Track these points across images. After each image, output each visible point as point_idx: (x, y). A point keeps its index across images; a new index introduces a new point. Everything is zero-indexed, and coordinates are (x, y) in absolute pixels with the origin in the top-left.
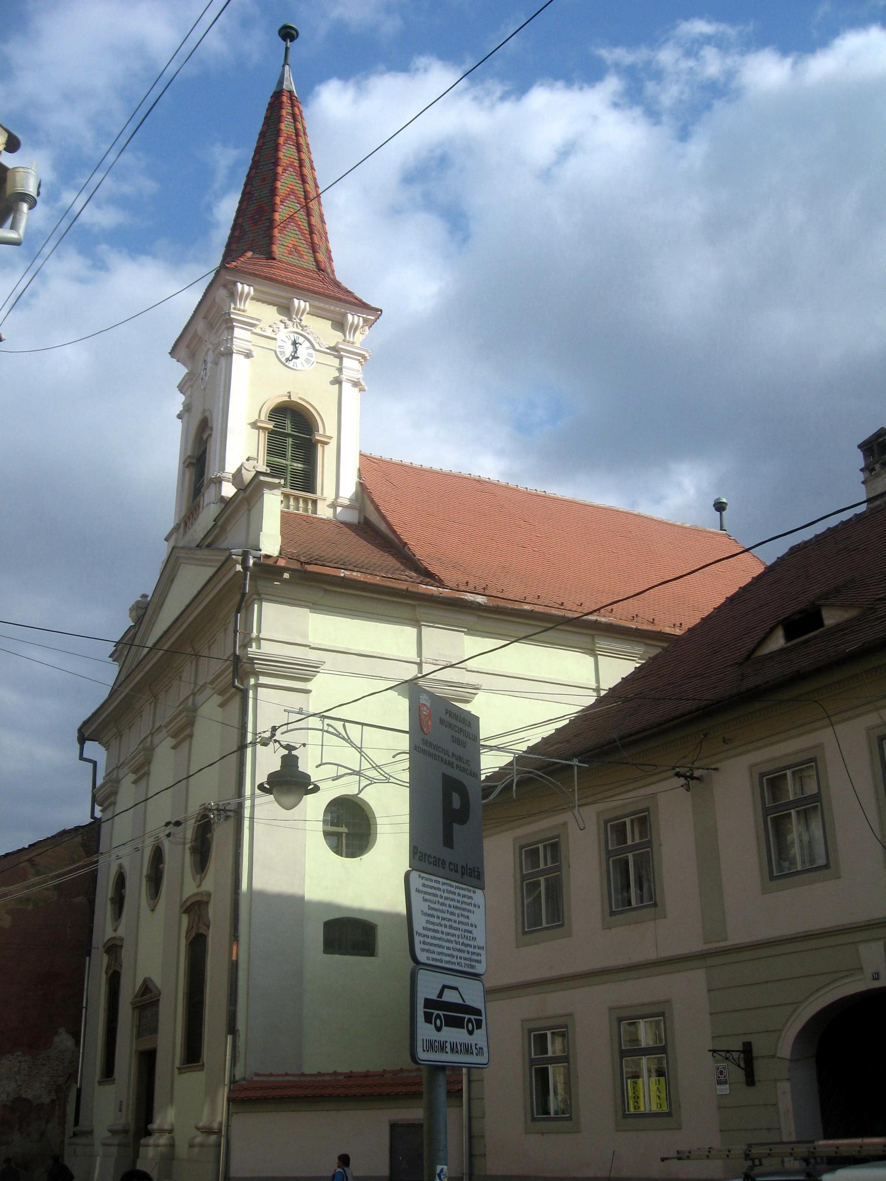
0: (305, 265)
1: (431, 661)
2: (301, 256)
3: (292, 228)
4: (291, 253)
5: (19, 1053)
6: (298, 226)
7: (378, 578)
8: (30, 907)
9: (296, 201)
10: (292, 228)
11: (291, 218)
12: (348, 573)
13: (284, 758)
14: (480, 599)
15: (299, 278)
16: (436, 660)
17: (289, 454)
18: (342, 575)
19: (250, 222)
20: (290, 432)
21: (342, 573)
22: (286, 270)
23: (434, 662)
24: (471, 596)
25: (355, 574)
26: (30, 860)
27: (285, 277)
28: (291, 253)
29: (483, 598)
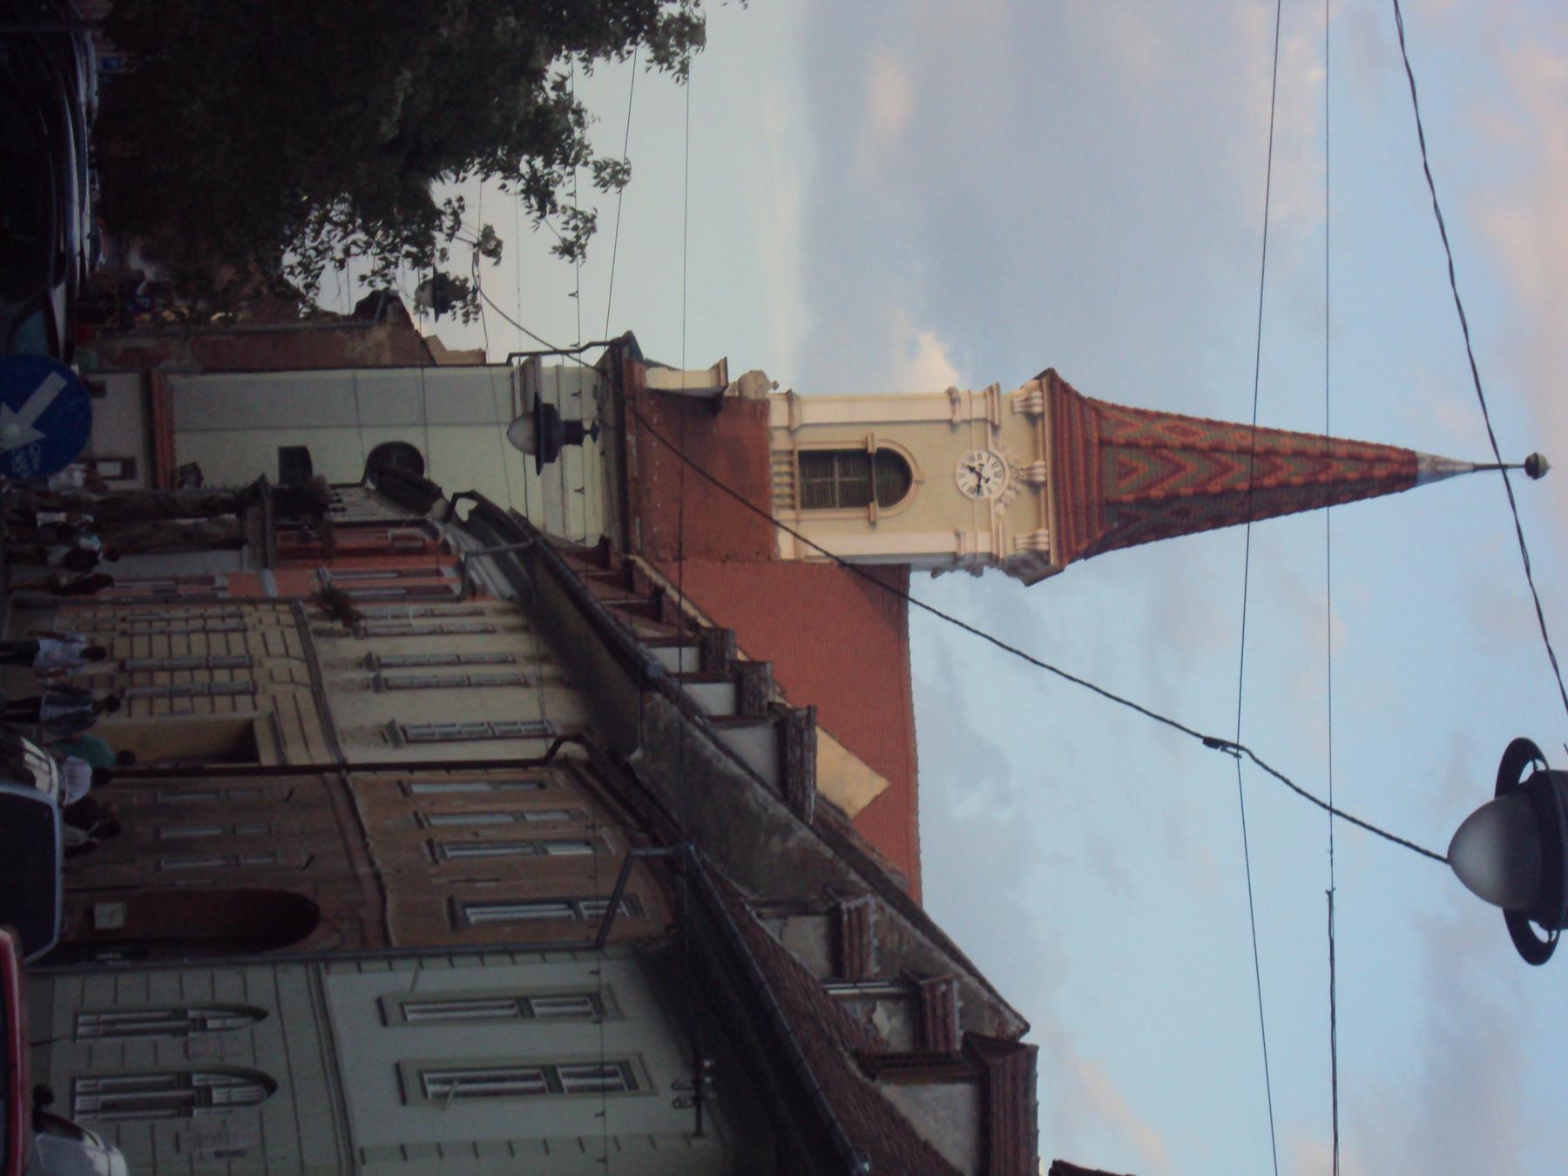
2: (1122, 477)
4: (1122, 464)
11: (1179, 468)
17: (846, 479)
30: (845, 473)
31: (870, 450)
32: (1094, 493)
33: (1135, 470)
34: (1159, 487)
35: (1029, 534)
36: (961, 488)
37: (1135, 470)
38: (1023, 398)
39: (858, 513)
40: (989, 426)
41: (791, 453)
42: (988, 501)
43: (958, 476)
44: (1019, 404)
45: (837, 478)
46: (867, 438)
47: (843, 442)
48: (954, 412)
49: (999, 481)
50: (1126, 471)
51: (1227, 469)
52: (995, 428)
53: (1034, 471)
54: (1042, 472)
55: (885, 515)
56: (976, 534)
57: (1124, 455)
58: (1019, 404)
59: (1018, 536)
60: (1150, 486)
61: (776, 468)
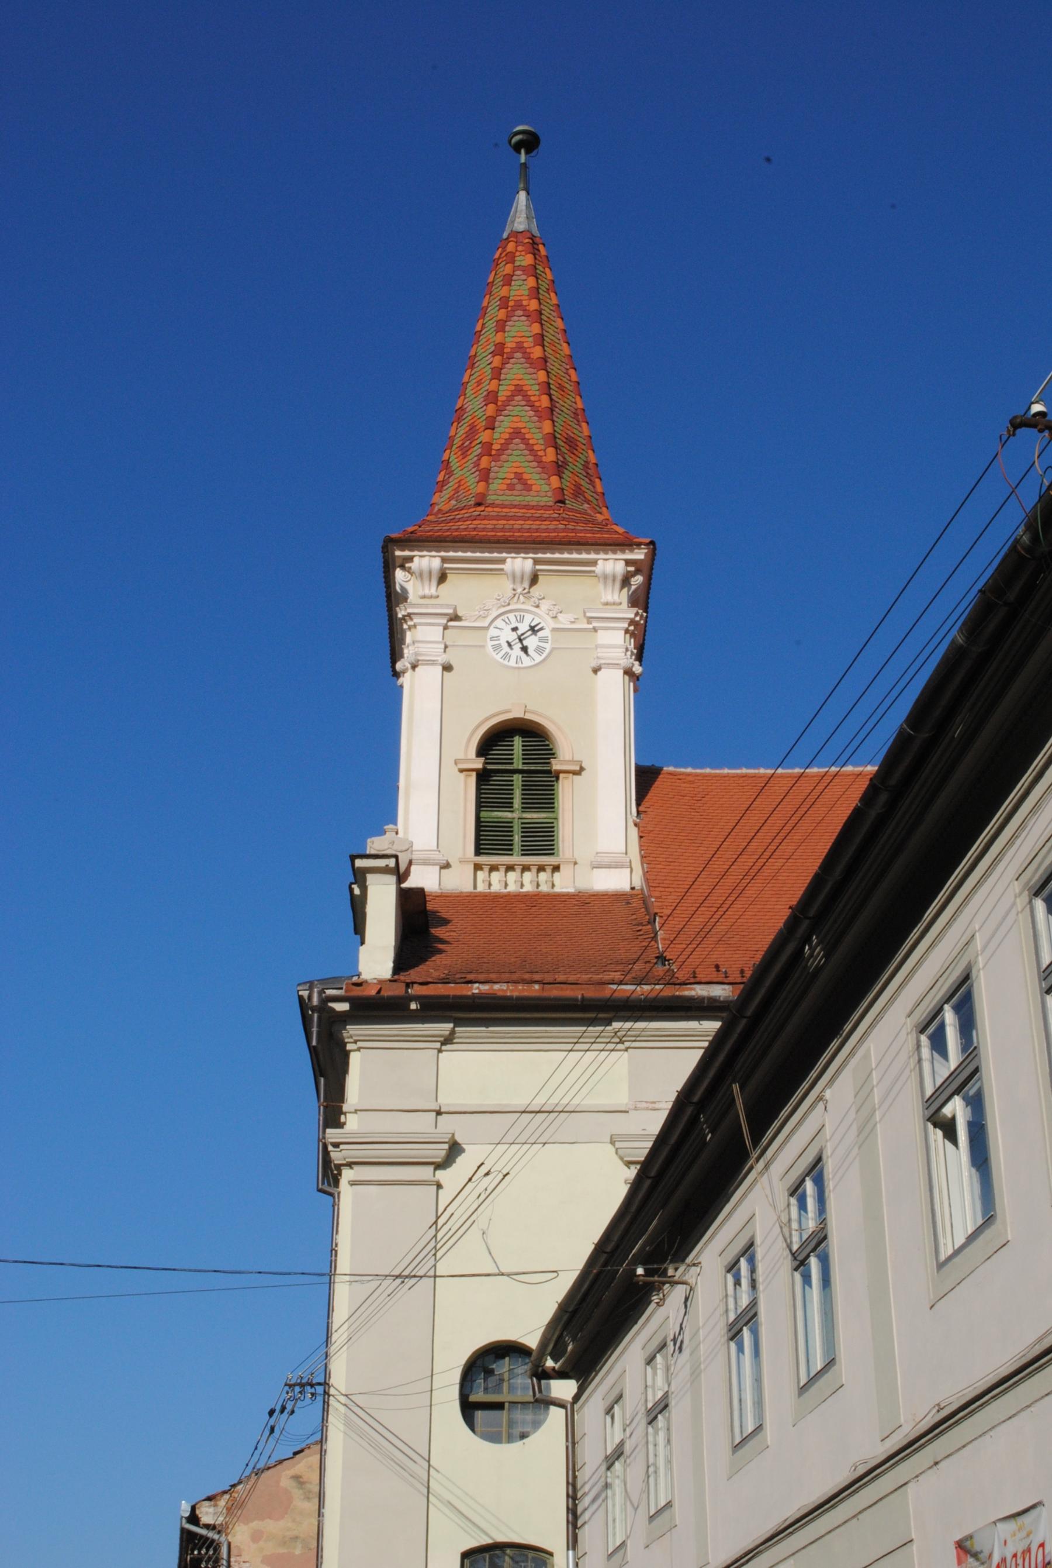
0: (531, 499)
1: (644, 1105)
2: (528, 487)
3: (515, 447)
4: (511, 487)
6: (525, 441)
7: (537, 987)
8: (298, 1552)
9: (524, 403)
10: (515, 447)
11: (517, 433)
12: (485, 988)
16: (654, 1103)
17: (517, 803)
18: (476, 991)
19: (460, 453)
20: (520, 767)
21: (476, 989)
22: (498, 518)
23: (651, 1106)
24: (701, 990)
25: (497, 987)
26: (297, 1478)
28: (511, 487)
29: (725, 989)
30: (508, 805)
32: (547, 514)
33: (519, 476)
35: (601, 586)
36: (536, 662)
39: (566, 791)
41: (478, 867)
42: (554, 630)
43: (520, 665)
45: (516, 815)
46: (461, 771)
47: (466, 799)
48: (433, 663)
50: (520, 481)
51: (519, 390)
52: (456, 618)
53: (518, 574)
54: (520, 563)
55: (566, 753)
56: (597, 647)
58: (427, 583)
59: (604, 600)
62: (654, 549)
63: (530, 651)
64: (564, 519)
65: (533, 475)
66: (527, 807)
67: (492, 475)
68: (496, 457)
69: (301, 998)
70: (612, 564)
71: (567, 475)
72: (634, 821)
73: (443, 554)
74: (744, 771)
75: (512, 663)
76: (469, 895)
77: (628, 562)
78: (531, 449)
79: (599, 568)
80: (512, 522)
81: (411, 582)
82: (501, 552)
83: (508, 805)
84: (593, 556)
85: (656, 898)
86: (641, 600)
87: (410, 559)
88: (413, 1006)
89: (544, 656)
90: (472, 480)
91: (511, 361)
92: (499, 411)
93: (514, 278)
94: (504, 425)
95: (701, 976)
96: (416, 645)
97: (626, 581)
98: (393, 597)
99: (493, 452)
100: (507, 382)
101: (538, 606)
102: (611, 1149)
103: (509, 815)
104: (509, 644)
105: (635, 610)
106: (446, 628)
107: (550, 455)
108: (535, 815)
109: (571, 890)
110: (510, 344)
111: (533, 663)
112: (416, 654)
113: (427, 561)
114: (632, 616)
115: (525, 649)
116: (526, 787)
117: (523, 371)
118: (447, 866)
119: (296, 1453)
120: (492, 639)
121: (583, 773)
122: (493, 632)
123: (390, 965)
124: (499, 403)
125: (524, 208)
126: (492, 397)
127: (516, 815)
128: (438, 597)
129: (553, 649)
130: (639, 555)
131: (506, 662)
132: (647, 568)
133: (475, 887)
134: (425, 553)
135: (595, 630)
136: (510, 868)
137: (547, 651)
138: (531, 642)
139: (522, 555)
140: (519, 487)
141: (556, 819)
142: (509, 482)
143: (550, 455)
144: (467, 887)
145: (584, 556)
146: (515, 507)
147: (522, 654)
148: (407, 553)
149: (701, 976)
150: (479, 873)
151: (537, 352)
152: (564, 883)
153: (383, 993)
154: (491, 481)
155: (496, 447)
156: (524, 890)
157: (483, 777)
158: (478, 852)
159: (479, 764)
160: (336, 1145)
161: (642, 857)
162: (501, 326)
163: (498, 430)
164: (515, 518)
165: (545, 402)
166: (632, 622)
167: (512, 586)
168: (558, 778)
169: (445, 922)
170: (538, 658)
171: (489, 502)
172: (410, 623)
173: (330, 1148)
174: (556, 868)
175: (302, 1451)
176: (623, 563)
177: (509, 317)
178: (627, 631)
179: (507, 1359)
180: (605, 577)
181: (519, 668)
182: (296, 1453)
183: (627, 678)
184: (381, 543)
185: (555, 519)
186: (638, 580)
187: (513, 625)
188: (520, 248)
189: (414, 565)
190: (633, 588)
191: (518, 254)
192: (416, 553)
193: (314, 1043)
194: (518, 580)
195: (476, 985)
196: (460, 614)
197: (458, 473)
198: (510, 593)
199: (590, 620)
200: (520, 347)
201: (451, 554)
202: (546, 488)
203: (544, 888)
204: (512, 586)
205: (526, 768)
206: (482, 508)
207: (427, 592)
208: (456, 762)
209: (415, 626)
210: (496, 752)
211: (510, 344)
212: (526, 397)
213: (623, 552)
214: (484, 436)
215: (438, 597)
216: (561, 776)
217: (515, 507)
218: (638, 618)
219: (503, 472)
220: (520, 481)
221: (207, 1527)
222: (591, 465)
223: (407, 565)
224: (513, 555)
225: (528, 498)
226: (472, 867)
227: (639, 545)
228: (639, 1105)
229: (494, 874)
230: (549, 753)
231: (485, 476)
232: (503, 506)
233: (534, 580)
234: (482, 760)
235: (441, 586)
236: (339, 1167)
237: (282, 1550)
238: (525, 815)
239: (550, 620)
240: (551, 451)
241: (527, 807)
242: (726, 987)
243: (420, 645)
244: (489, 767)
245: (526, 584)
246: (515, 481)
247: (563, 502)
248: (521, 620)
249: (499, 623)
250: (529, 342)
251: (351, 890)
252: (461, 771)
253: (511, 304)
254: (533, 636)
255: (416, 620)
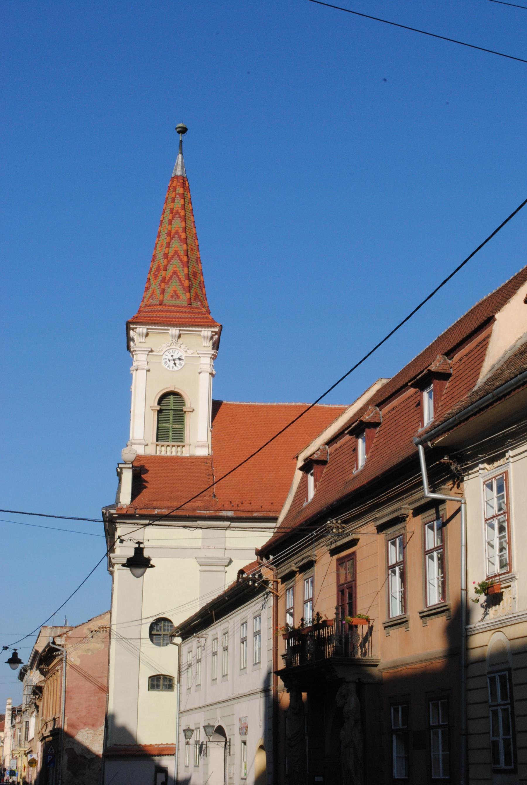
0: (179, 303)
1: (206, 547)
2: (178, 297)
4: (172, 297)
5: (87, 729)
6: (178, 276)
8: (90, 654)
11: (175, 273)
12: (159, 511)
13: (13, 653)
14: (230, 514)
15: (174, 315)
17: (171, 421)
20: (173, 408)
22: (167, 311)
25: (163, 510)
27: (165, 317)
30: (168, 422)
31: (159, 409)
33: (175, 292)
34: (183, 282)
35: (203, 340)
36: (179, 368)
37: (175, 292)
38: (138, 336)
39: (188, 418)
40: (150, 353)
41: (157, 445)
42: (186, 357)
43: (173, 370)
44: (141, 339)
45: (170, 426)
46: (152, 410)
47: (154, 421)
48: (143, 369)
49: (177, 351)
50: (175, 295)
51: (176, 253)
52: (152, 351)
53: (174, 335)
54: (174, 331)
55: (189, 404)
56: (200, 364)
57: (167, 296)
58: (141, 339)
60: (182, 285)
61: (163, 454)
62: (222, 328)
63: (177, 364)
64: (191, 313)
65: (181, 292)
66: (175, 422)
67: (165, 291)
68: (167, 283)
69: (103, 512)
70: (207, 332)
71: (193, 290)
72: (210, 430)
73: (147, 327)
74: (251, 403)
75: (171, 369)
76: (155, 456)
77: (212, 332)
78: (179, 279)
79: (202, 333)
80: (172, 314)
81: (136, 336)
82: (168, 327)
83: (168, 422)
84: (200, 329)
85: (215, 468)
86: (216, 346)
87: (136, 328)
88: (137, 516)
89: (182, 366)
90: (158, 292)
91: (174, 239)
92: (169, 262)
93: (176, 198)
94: (171, 269)
95: (226, 507)
96: (137, 362)
97: (211, 338)
98: (129, 339)
99: (166, 281)
100: (173, 249)
101: (180, 347)
102: (195, 560)
103: (168, 425)
104: (169, 360)
105: (214, 351)
106: (148, 355)
107: (186, 283)
108: (177, 426)
109: (188, 455)
110: (173, 231)
111: (178, 369)
112: (138, 366)
113: (142, 329)
114: (213, 353)
115: (175, 364)
116: (174, 415)
117: (178, 244)
118: (147, 445)
119: (89, 621)
120: (164, 359)
121: (194, 412)
122: (164, 357)
123: (130, 500)
124: (169, 259)
125: (181, 163)
126: (166, 256)
127: (170, 426)
128: (145, 342)
129: (185, 364)
130: (217, 329)
131: (168, 369)
132: (219, 333)
133: (156, 453)
134: (141, 326)
135: (200, 357)
136: (168, 446)
137: (183, 365)
138: (177, 362)
139: (175, 328)
140: (175, 297)
141: (184, 427)
142: (171, 294)
143: (186, 283)
144: (153, 454)
145: (197, 329)
146: (173, 306)
147: (174, 365)
148: (135, 326)
149: (226, 507)
150: (158, 447)
151: (183, 236)
152: (186, 452)
153: (127, 513)
154: (165, 294)
155: (167, 278)
156: (172, 455)
157: (160, 412)
158: (157, 441)
159: (158, 408)
160: (113, 558)
161: (212, 442)
162: (170, 223)
163: (168, 271)
164: (173, 312)
165: (185, 259)
166: (213, 355)
167: (171, 339)
168: (185, 413)
169: (147, 482)
170: (180, 367)
171: (164, 304)
172: (136, 353)
173: (112, 559)
174: (184, 446)
175: (91, 620)
176: (211, 332)
177: (173, 217)
178: (211, 358)
179: (163, 622)
180: (204, 337)
181: (173, 371)
182: (89, 621)
183: (210, 375)
184: (126, 322)
185: (187, 313)
186: (216, 337)
187: (172, 355)
188: (178, 184)
189: (137, 330)
190: (214, 340)
191: (177, 187)
192: (138, 326)
193: (107, 528)
194: (174, 337)
195: (156, 510)
196: (153, 350)
197: (153, 286)
198: (171, 342)
199: (198, 354)
200: (177, 232)
201: (150, 327)
202: (185, 298)
203: (179, 454)
204: (171, 339)
205: (174, 409)
206: (161, 307)
207: (141, 340)
208: (151, 407)
209: (137, 354)
210: (165, 401)
211: (173, 231)
212: (179, 256)
213: (211, 328)
214: (162, 273)
215: (145, 342)
216: (186, 412)
217: (173, 306)
218: (215, 353)
219: (169, 290)
220: (175, 295)
221: (60, 645)
222: (202, 282)
223: (135, 330)
224: (172, 328)
225: (178, 302)
226: (155, 445)
227: (216, 326)
228: (204, 547)
229: (163, 448)
230: (183, 403)
231: (163, 292)
232: (169, 306)
233: (179, 336)
234: (160, 406)
235: (147, 338)
236: (114, 564)
237: (84, 653)
238: (174, 426)
239: (184, 353)
240: (187, 281)
241: (175, 422)
242: (232, 512)
243: (139, 362)
244: (162, 408)
245: (176, 339)
246: (174, 294)
247: (191, 304)
248: (174, 352)
249: (167, 353)
250: (181, 230)
251: (117, 470)
252: (152, 410)
253: (174, 211)
254: (179, 361)
255: (137, 352)
